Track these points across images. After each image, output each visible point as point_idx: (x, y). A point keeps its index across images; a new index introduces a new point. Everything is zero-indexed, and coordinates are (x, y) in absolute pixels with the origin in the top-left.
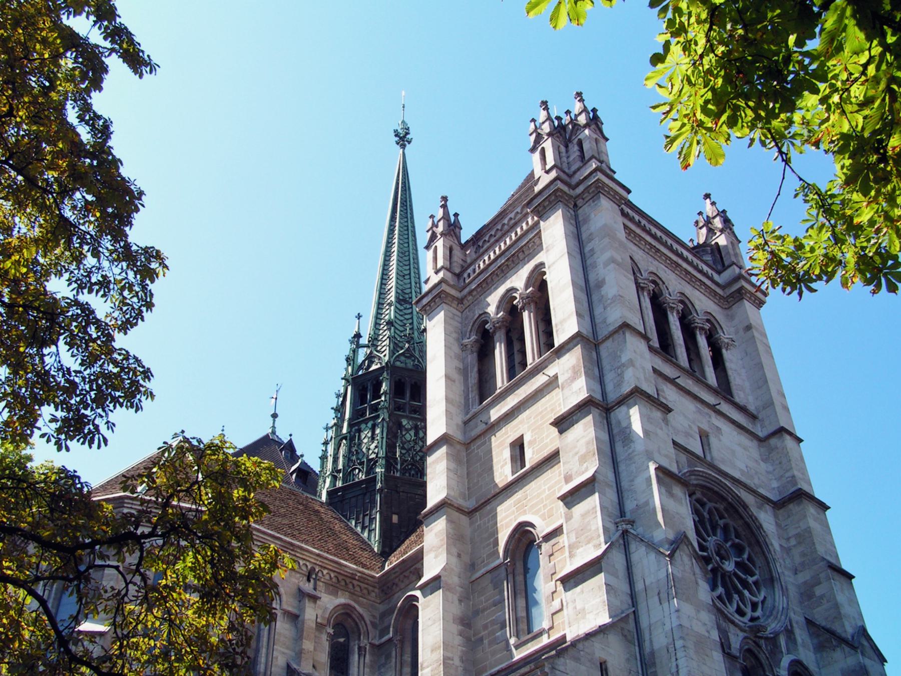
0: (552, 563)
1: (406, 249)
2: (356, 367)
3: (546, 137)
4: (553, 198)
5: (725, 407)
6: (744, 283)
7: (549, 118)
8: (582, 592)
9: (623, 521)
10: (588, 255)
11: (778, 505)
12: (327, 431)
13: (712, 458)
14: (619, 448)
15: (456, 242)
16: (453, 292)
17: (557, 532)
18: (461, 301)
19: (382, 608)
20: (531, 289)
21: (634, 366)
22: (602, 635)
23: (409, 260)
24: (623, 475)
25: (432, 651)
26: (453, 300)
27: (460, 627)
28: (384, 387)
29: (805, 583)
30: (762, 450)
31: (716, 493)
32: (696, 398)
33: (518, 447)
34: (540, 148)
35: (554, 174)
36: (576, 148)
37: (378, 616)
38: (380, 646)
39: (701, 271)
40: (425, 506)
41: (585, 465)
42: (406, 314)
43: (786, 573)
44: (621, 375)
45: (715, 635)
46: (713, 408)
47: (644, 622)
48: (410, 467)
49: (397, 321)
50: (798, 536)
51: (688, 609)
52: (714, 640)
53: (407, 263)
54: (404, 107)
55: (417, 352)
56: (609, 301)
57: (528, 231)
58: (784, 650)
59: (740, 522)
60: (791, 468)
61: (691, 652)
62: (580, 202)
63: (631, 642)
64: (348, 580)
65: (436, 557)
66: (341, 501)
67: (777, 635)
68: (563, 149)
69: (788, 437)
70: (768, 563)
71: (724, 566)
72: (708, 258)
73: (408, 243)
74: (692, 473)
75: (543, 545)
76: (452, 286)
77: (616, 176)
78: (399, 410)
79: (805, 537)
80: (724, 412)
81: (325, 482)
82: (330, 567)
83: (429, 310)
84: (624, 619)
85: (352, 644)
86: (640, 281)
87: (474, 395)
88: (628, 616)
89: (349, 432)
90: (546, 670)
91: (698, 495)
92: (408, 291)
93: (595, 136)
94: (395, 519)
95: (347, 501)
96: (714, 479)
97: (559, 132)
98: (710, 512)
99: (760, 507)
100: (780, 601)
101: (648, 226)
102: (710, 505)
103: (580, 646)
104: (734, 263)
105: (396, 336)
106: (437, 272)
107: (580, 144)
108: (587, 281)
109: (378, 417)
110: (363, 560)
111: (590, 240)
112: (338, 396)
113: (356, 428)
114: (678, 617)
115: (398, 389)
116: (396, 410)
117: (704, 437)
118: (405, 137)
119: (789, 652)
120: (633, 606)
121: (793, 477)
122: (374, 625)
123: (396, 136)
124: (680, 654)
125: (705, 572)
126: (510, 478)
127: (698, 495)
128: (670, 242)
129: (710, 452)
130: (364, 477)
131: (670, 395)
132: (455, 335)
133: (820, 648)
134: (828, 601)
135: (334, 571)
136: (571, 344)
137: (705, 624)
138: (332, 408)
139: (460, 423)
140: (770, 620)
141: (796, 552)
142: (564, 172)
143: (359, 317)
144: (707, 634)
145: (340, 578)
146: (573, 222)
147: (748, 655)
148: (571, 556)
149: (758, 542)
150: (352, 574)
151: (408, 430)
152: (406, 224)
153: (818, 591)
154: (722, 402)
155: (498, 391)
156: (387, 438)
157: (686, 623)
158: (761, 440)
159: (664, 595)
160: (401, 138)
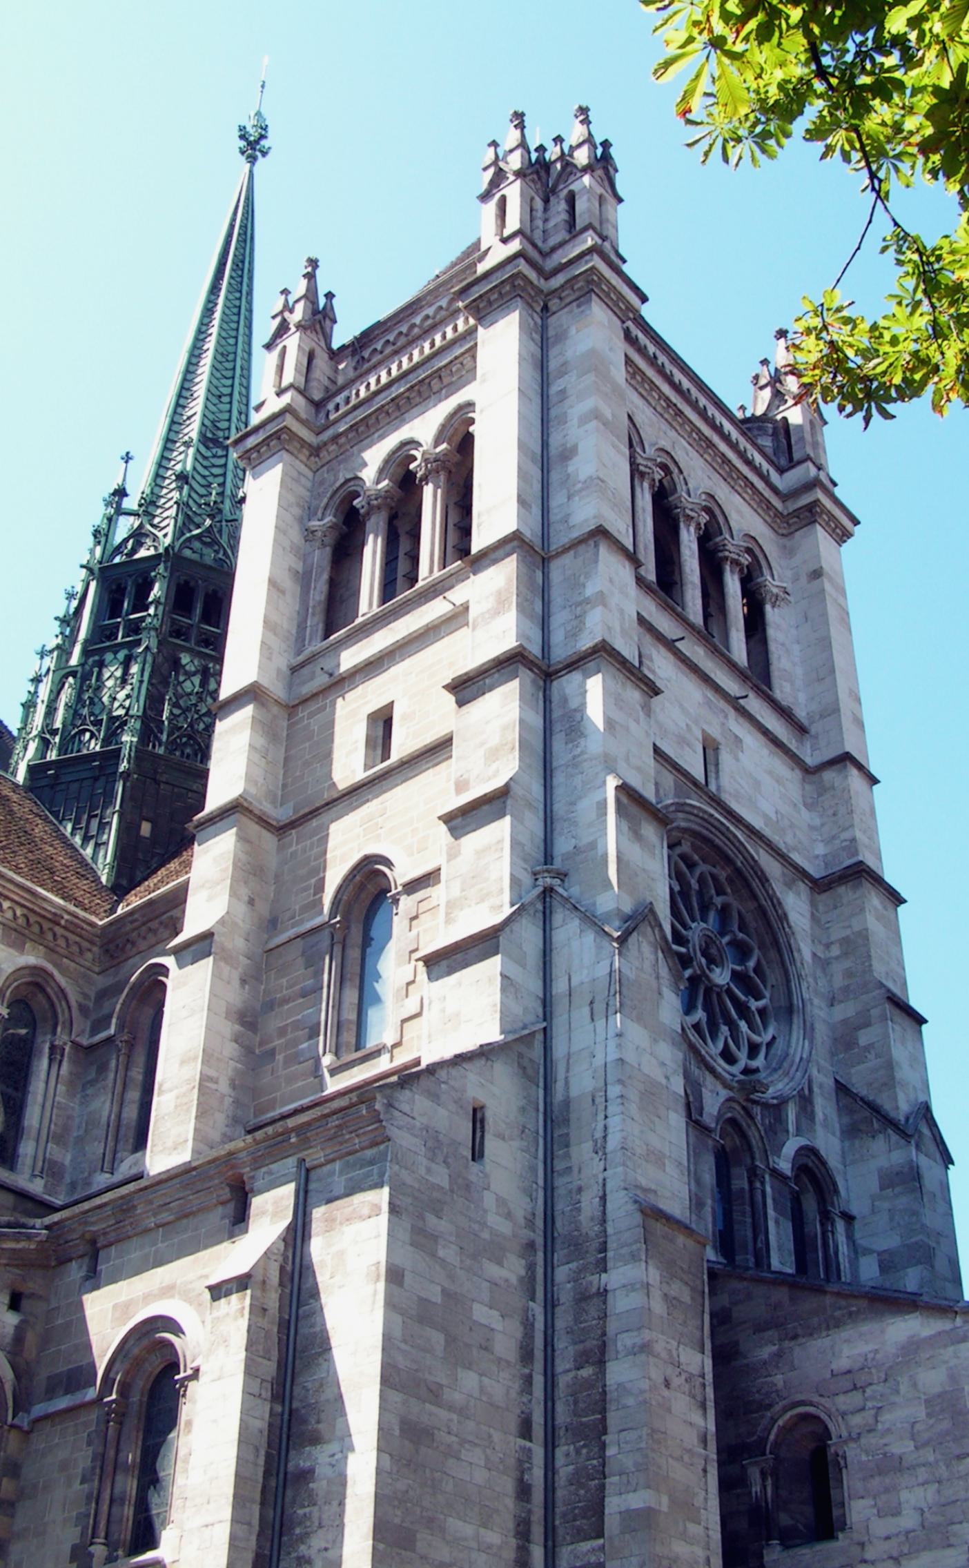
0: (414, 932)
1: (231, 349)
2: (110, 549)
3: (512, 178)
4: (508, 288)
5: (754, 705)
6: (819, 494)
7: (523, 144)
8: (460, 984)
9: (547, 871)
10: (553, 399)
11: (821, 886)
12: (42, 658)
13: (719, 788)
14: (558, 744)
15: (323, 344)
16: (304, 433)
17: (428, 879)
18: (315, 451)
19: (102, 982)
20: (444, 446)
21: (605, 605)
22: (483, 1062)
23: (234, 369)
24: (559, 792)
25: (183, 1063)
26: (302, 447)
27: (237, 1027)
28: (156, 591)
29: (845, 1022)
30: (807, 787)
32: (706, 679)
33: (383, 722)
34: (497, 196)
35: (515, 246)
36: (563, 206)
37: (93, 996)
38: (92, 1048)
39: (749, 463)
40: (203, 809)
41: (494, 766)
42: (214, 466)
43: (816, 1001)
44: (580, 618)
45: (678, 1085)
46: (734, 702)
47: (559, 1050)
48: (184, 740)
49: (198, 477)
50: (845, 941)
51: (638, 1035)
52: (675, 1093)
53: (229, 374)
54: (263, 86)
55: (225, 537)
56: (579, 486)
57: (454, 342)
58: (791, 1128)
59: (752, 905)
60: (852, 826)
61: (633, 1109)
62: (554, 304)
63: (532, 1080)
64: (46, 925)
65: (210, 899)
66: (52, 787)
67: (783, 1101)
68: (539, 204)
69: (854, 772)
70: (788, 981)
71: (712, 976)
72: (766, 442)
73: (236, 338)
74: (680, 807)
75: (404, 900)
76: (304, 422)
77: (625, 268)
78: (178, 637)
79: (857, 945)
80: (752, 712)
81: (26, 748)
82: (16, 898)
83: (255, 459)
84: (527, 1040)
85: (39, 1039)
86: (639, 460)
87: (316, 621)
88: (532, 1034)
89: (82, 665)
90: (377, 1107)
91: (686, 847)
92: (224, 425)
93: (600, 190)
94: (146, 829)
95: (63, 787)
96: (716, 823)
97: (537, 173)
98: (701, 880)
99: (789, 885)
100: (798, 1046)
101: (669, 367)
102: (703, 868)
103: (442, 1074)
104: (808, 458)
105: (191, 502)
106: (279, 394)
107: (571, 199)
108: (545, 445)
109: (138, 643)
110: (79, 894)
111: (562, 373)
112: (70, 596)
113: (97, 658)
114: (619, 1046)
115: (181, 598)
116: (171, 636)
117: (710, 750)
118: (257, 142)
119: (799, 1132)
120: (545, 1020)
121: (853, 840)
122: (83, 1009)
123: (242, 137)
124: (612, 1109)
125: (677, 977)
126: (360, 775)
127: (686, 847)
128: (703, 401)
129: (717, 778)
130: (98, 749)
131: (662, 667)
132: (297, 511)
133: (851, 1132)
134: (877, 1056)
135: (23, 906)
136: (501, 552)
137: (663, 1064)
138: (56, 618)
139: (285, 669)
140: (776, 1076)
141: (838, 969)
142: (534, 245)
143: (127, 458)
144: (664, 1081)
145: (33, 918)
146: (537, 337)
147: (729, 1129)
148: (449, 920)
149: (776, 943)
150: (55, 914)
151: (189, 675)
152: (237, 303)
153: (864, 1038)
154: (752, 695)
155: (359, 620)
156: (150, 682)
157: (631, 1057)
158: (809, 771)
159: (600, 1007)
160: (249, 143)
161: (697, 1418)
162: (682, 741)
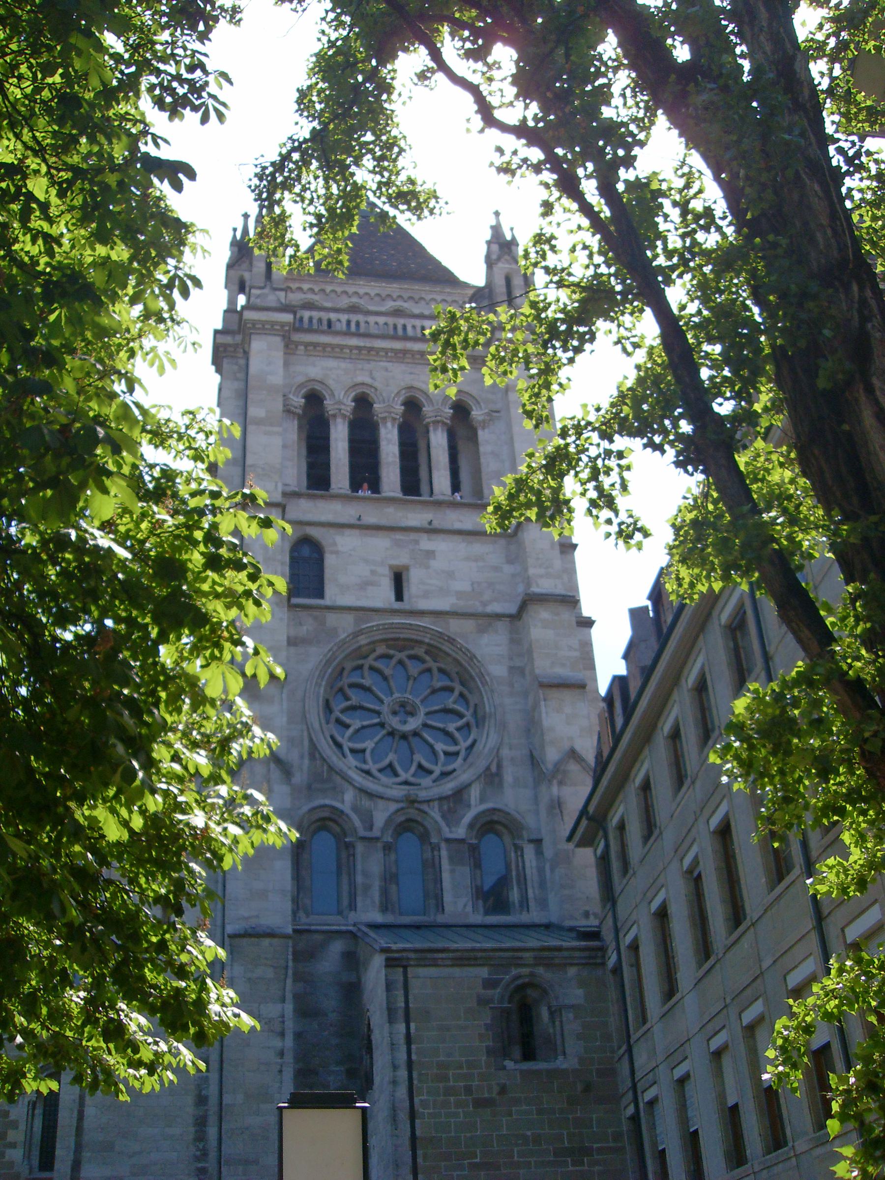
31: (404, 639)
161: (277, 1043)
162: (364, 585)
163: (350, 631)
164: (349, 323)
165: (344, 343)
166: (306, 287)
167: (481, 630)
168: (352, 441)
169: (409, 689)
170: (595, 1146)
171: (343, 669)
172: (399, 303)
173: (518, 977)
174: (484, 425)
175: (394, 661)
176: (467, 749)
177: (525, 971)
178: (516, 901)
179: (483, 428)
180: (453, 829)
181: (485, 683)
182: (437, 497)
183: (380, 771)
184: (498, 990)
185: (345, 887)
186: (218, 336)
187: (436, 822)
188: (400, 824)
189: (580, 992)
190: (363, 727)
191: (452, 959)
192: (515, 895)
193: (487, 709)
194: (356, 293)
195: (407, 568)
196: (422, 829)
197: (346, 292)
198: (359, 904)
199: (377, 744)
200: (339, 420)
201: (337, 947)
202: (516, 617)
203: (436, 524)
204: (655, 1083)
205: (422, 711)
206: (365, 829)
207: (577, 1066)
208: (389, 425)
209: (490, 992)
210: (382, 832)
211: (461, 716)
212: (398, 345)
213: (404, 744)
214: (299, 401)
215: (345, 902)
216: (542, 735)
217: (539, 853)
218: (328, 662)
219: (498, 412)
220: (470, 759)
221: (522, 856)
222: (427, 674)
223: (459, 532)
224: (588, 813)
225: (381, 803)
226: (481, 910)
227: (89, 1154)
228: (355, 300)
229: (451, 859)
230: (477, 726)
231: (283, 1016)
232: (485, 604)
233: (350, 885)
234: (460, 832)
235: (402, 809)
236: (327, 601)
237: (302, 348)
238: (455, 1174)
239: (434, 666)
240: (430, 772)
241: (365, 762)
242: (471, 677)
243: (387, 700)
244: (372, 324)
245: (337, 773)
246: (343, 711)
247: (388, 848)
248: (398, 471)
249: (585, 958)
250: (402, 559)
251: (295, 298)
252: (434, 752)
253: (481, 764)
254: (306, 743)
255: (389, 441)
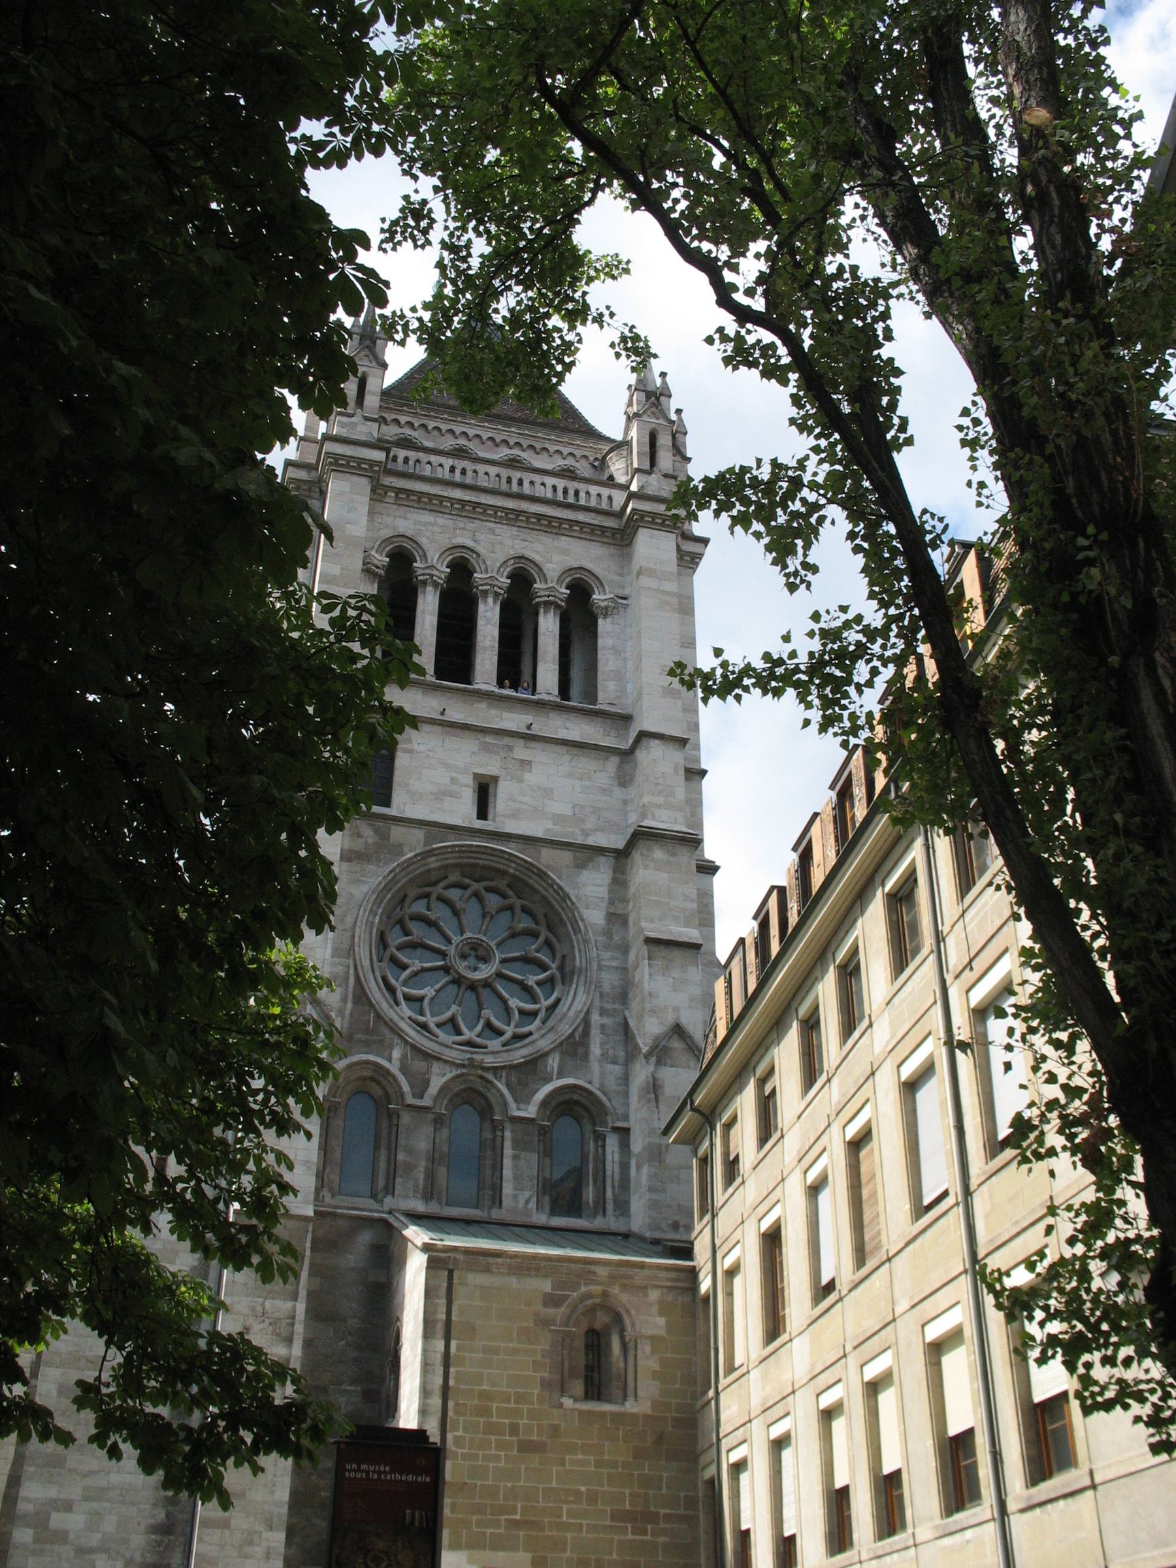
31: (484, 867)
102: (476, 886)
162: (442, 794)
163: (418, 851)
164: (452, 469)
165: (445, 494)
166: (403, 419)
167: (581, 865)
168: (441, 615)
169: (484, 927)
170: (662, 1511)
171: (405, 896)
172: (516, 452)
173: (588, 1296)
174: (606, 613)
175: (469, 892)
176: (547, 1009)
177: (596, 1289)
178: (591, 1201)
179: (605, 616)
180: (522, 1106)
181: (577, 930)
182: (541, 696)
183: (439, 1025)
184: (563, 1309)
185: (383, 1165)
186: (290, 468)
187: (502, 1095)
188: (457, 1095)
189: (662, 1321)
190: (423, 970)
191: (510, 1267)
192: (589, 1194)
193: (578, 964)
194: (464, 433)
195: (495, 779)
196: (483, 1102)
197: (451, 431)
198: (398, 1189)
199: (437, 991)
200: (429, 589)
201: (365, 1238)
202: (622, 855)
203: (536, 730)
204: (745, 1441)
205: (498, 956)
206: (414, 1096)
207: (649, 1412)
208: (490, 600)
209: (551, 1311)
210: (435, 1102)
211: (544, 968)
212: (510, 504)
213: (470, 997)
214: (382, 559)
215: (381, 1183)
216: (643, 1000)
217: (625, 1145)
218: (387, 887)
219: (625, 599)
220: (550, 1023)
221: (604, 1147)
222: (508, 914)
223: (565, 743)
224: (692, 1102)
225: (436, 1067)
226: (547, 1209)
227: (32, 1469)
228: (462, 441)
229: (516, 1144)
230: (563, 984)
231: (293, 1317)
232: (586, 834)
233: (389, 1163)
234: (530, 1111)
235: (462, 1075)
236: (392, 811)
237: (393, 494)
238: (489, 1531)
239: (518, 903)
240: (501, 1033)
241: (422, 1013)
242: (561, 920)
243: (456, 939)
244: (481, 474)
245: (385, 1022)
246: (400, 948)
247: (438, 1121)
248: (496, 659)
249: (673, 1280)
250: (490, 766)
251: (391, 432)
252: (508, 1010)
253: (565, 1029)
254: (352, 980)
255: (488, 621)
